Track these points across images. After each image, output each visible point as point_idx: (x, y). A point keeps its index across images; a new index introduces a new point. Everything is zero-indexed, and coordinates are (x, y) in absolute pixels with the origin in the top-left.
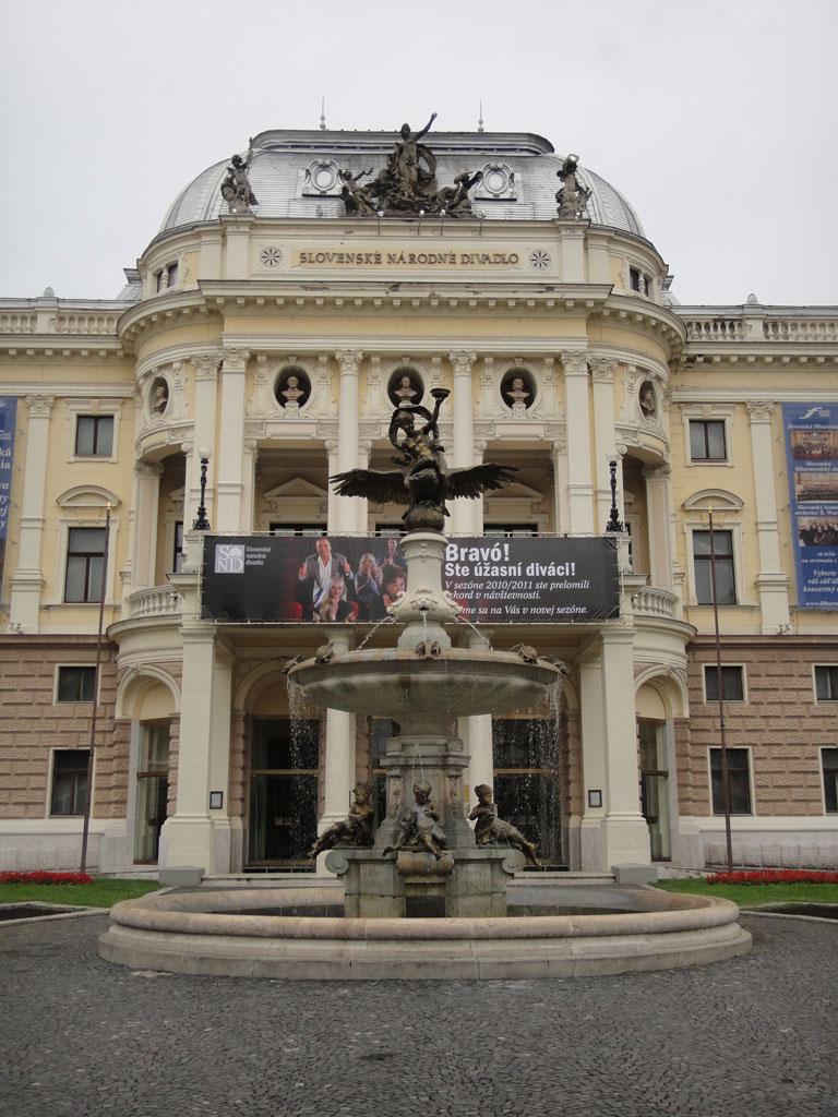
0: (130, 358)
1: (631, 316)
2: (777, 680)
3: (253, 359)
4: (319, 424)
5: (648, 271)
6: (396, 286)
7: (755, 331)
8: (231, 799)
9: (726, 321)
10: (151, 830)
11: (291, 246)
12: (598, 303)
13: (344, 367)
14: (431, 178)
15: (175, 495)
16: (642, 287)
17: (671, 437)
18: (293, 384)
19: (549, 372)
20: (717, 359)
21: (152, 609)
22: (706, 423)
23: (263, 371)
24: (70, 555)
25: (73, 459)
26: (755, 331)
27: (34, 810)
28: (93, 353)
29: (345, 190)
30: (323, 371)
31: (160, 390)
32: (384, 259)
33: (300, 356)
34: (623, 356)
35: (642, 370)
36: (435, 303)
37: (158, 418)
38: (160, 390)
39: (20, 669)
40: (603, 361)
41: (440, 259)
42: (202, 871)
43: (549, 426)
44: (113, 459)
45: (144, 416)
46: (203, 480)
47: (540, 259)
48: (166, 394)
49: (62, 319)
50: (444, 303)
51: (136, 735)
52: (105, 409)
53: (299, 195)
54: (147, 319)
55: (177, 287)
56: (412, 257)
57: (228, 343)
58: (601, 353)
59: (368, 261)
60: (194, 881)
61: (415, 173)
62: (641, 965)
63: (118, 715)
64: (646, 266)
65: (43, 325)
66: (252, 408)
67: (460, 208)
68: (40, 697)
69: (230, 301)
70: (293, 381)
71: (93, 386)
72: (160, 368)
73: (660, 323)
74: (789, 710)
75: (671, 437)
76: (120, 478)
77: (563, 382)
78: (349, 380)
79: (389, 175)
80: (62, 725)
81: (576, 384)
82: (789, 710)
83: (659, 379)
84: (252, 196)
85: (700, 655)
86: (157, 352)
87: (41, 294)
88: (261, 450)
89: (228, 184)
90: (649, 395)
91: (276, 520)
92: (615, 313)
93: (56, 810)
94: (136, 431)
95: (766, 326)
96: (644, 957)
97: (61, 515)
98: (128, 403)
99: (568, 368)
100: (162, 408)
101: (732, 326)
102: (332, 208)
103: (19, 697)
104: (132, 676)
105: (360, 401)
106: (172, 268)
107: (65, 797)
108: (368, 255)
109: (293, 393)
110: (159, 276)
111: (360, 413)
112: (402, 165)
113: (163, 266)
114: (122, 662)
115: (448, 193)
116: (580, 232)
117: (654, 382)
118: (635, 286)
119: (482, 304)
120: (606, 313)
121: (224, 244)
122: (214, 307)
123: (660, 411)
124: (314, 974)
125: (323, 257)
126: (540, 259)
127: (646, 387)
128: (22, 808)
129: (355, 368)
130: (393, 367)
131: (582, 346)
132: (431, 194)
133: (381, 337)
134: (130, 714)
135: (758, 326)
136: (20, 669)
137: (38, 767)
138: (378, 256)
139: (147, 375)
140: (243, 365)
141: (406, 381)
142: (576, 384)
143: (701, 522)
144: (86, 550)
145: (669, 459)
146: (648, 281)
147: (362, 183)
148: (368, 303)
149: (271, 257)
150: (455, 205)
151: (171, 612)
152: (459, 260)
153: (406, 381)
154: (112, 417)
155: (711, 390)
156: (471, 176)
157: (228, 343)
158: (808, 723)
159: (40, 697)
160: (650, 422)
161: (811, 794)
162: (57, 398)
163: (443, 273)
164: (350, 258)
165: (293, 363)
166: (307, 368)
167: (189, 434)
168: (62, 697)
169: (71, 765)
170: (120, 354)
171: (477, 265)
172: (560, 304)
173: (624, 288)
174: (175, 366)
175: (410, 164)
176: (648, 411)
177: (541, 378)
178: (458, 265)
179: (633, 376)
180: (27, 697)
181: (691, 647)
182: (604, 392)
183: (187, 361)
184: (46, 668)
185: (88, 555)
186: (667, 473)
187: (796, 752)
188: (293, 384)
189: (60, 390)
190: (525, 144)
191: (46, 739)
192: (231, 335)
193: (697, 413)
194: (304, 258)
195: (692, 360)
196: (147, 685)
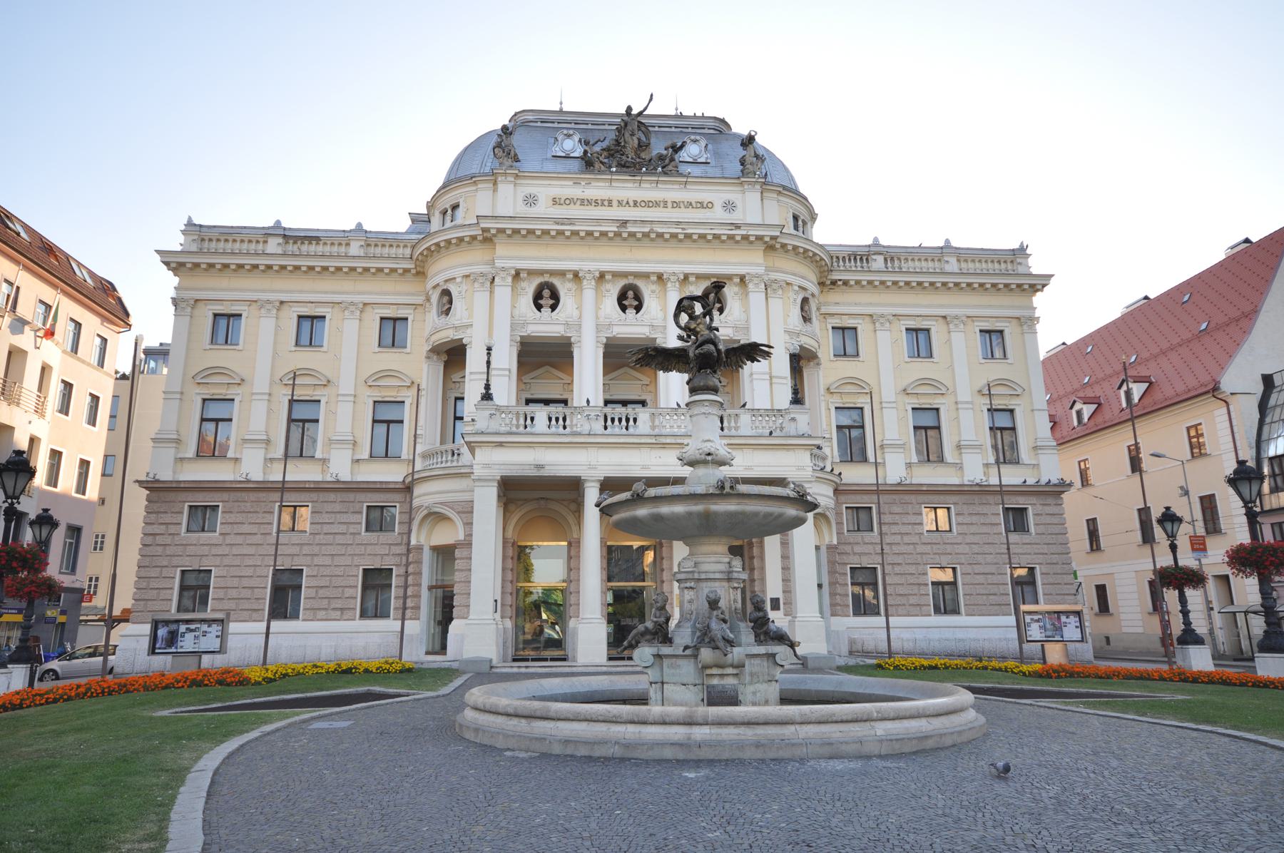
0: (421, 274)
1: (795, 248)
2: (897, 517)
3: (517, 275)
4: (567, 324)
5: (803, 218)
6: (624, 223)
7: (878, 262)
8: (503, 605)
9: (860, 256)
10: (439, 629)
11: (545, 191)
12: (773, 238)
13: (585, 282)
14: (648, 145)
15: (456, 377)
16: (801, 229)
18: (547, 296)
19: (736, 289)
20: (852, 283)
21: (440, 464)
22: (843, 329)
23: (524, 284)
24: (374, 421)
25: (377, 349)
26: (878, 262)
27: (350, 613)
28: (393, 270)
29: (585, 152)
30: (569, 285)
31: (446, 299)
32: (615, 203)
33: (553, 273)
34: (790, 278)
35: (803, 288)
36: (653, 236)
37: (443, 319)
38: (446, 299)
39: (338, 507)
40: (775, 281)
41: (657, 204)
42: (491, 661)
43: (735, 328)
44: (408, 350)
45: (432, 315)
46: (488, 363)
47: (729, 206)
48: (450, 302)
49: (369, 245)
50: (660, 235)
51: (427, 556)
52: (401, 313)
53: (549, 156)
54: (437, 245)
55: (459, 221)
56: (635, 203)
57: (499, 263)
58: (774, 276)
59: (603, 205)
60: (485, 668)
61: (636, 141)
62: (930, 744)
63: (413, 542)
64: (803, 214)
65: (355, 249)
66: (516, 312)
67: (670, 167)
68: (352, 529)
69: (501, 231)
70: (546, 293)
71: (391, 295)
72: (446, 281)
73: (815, 254)
74: (906, 539)
75: (823, 341)
76: (414, 363)
77: (747, 294)
78: (589, 293)
79: (618, 143)
80: (369, 549)
81: (756, 296)
82: (906, 539)
83: (813, 295)
84: (516, 155)
85: (842, 498)
86: (445, 269)
87: (353, 227)
88: (522, 344)
89: (499, 145)
90: (806, 308)
91: (530, 397)
92: (784, 246)
93: (363, 615)
94: (426, 329)
95: (886, 260)
96: (931, 736)
97: (369, 392)
98: (420, 310)
99: (751, 286)
100: (447, 312)
101: (861, 259)
102: (576, 165)
103: (335, 528)
104: (425, 512)
105: (598, 308)
106: (455, 207)
107: (370, 604)
108: (603, 201)
109: (546, 302)
110: (444, 213)
111: (597, 318)
112: (627, 135)
113: (448, 206)
114: (416, 503)
115: (661, 158)
116: (758, 187)
117: (811, 300)
118: (796, 228)
119: (688, 236)
120: (778, 246)
121: (495, 190)
122: (489, 235)
123: (814, 319)
124: (668, 753)
125: (570, 201)
126: (729, 206)
127: (805, 301)
128: (339, 613)
129: (593, 283)
130: (621, 283)
131: (761, 270)
132: (647, 158)
133: (613, 261)
134: (423, 541)
135: (880, 259)
136: (338, 507)
137: (351, 582)
138: (610, 202)
139: (434, 287)
140: (510, 279)
141: (630, 294)
142: (756, 296)
143: (838, 401)
144: (386, 420)
145: (820, 355)
146: (804, 223)
147: (597, 148)
148: (604, 234)
149: (531, 200)
150: (666, 165)
151: (455, 464)
152: (670, 205)
153: (630, 294)
154: (406, 319)
155: (846, 305)
156: (679, 144)
157: (499, 263)
158: (920, 549)
159: (352, 529)
160: (808, 327)
161: (923, 600)
162: (365, 304)
163: (659, 214)
164: (589, 202)
165: (546, 278)
166: (556, 282)
167: (469, 331)
168: (367, 530)
169: (376, 580)
170: (413, 271)
171: (683, 209)
172: (745, 238)
173: (790, 229)
174: (458, 280)
175: (632, 135)
177: (729, 292)
178: (669, 209)
179: (797, 293)
180: (343, 528)
181: (836, 491)
182: (776, 304)
183: (467, 276)
184: (357, 506)
185: (389, 422)
186: (818, 364)
187: (912, 569)
188: (547, 296)
189: (367, 299)
190: (712, 124)
191: (357, 560)
192: (501, 258)
193: (837, 322)
194: (555, 201)
195: (834, 283)
196: (435, 517)
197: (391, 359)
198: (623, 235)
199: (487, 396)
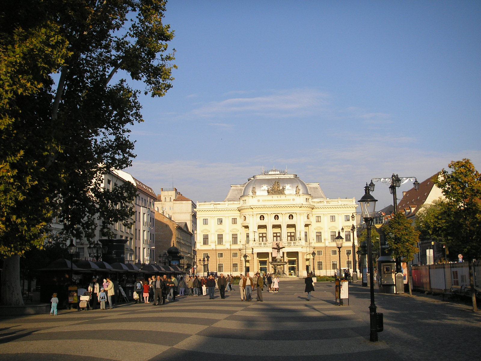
11: (261, 199)
17: (313, 219)
18: (262, 217)
57: (254, 213)
70: (262, 217)
81: (298, 216)
109: (262, 218)
135: (325, 202)
141: (276, 216)
142: (298, 216)
144: (235, 238)
149: (259, 201)
153: (276, 216)
157: (254, 213)
176: (308, 218)
188: (262, 217)
197: (235, 226)
198: (275, 207)
199: (255, 241)
